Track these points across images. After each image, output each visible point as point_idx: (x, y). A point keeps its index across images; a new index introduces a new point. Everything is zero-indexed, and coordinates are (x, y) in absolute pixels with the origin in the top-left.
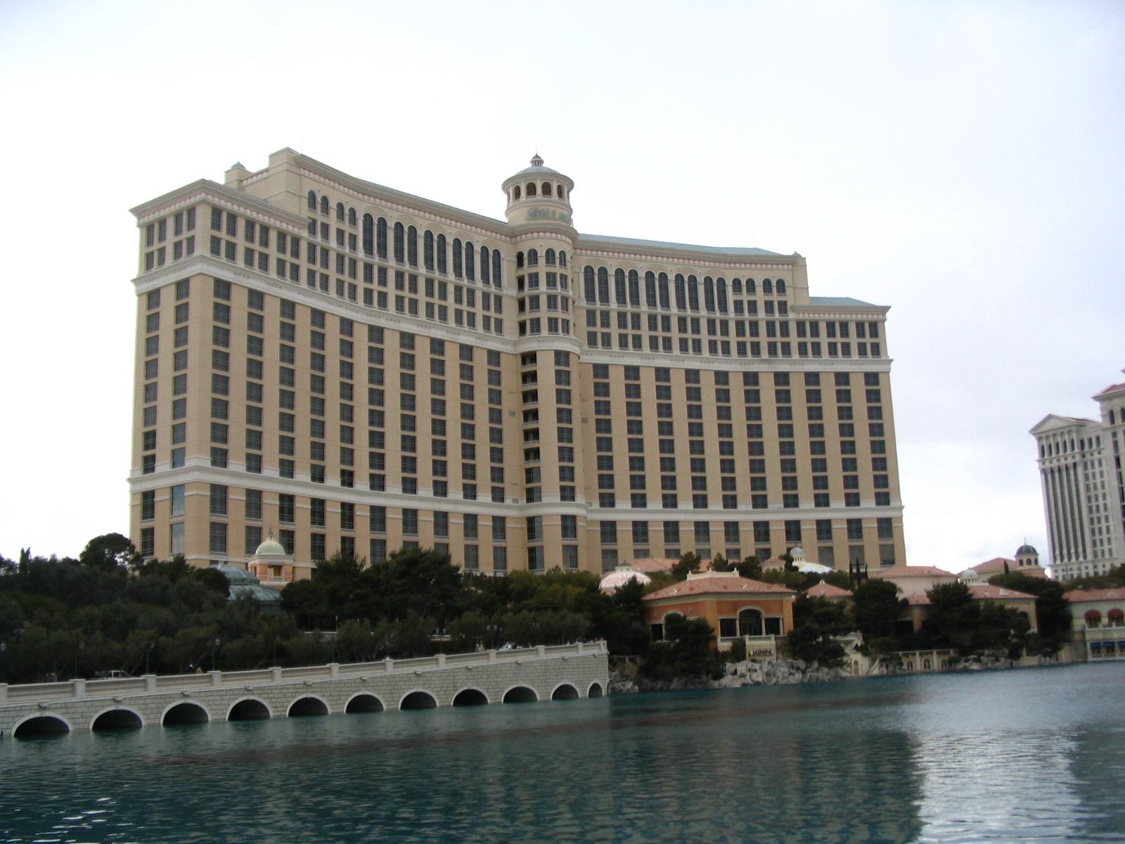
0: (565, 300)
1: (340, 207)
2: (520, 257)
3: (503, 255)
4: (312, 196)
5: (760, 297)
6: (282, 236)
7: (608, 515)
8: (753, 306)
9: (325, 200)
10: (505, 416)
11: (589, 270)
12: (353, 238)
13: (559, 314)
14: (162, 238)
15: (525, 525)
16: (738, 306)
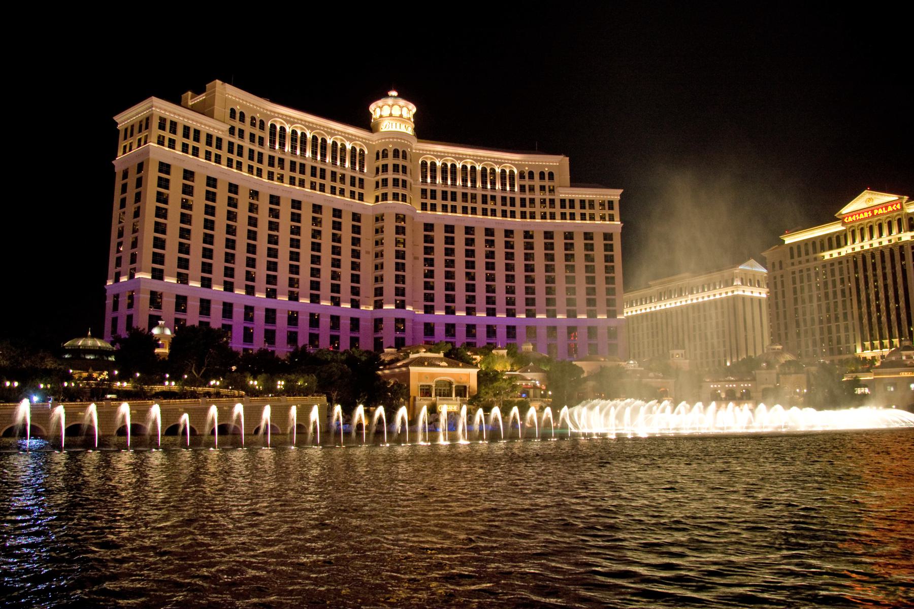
0: (404, 182)
1: (253, 119)
2: (378, 154)
3: (366, 152)
4: (233, 111)
5: (537, 182)
6: (209, 137)
7: (429, 318)
8: (532, 189)
9: (242, 115)
10: (362, 254)
11: (424, 164)
12: (261, 140)
13: (400, 191)
14: (132, 135)
15: (373, 323)
16: (522, 188)
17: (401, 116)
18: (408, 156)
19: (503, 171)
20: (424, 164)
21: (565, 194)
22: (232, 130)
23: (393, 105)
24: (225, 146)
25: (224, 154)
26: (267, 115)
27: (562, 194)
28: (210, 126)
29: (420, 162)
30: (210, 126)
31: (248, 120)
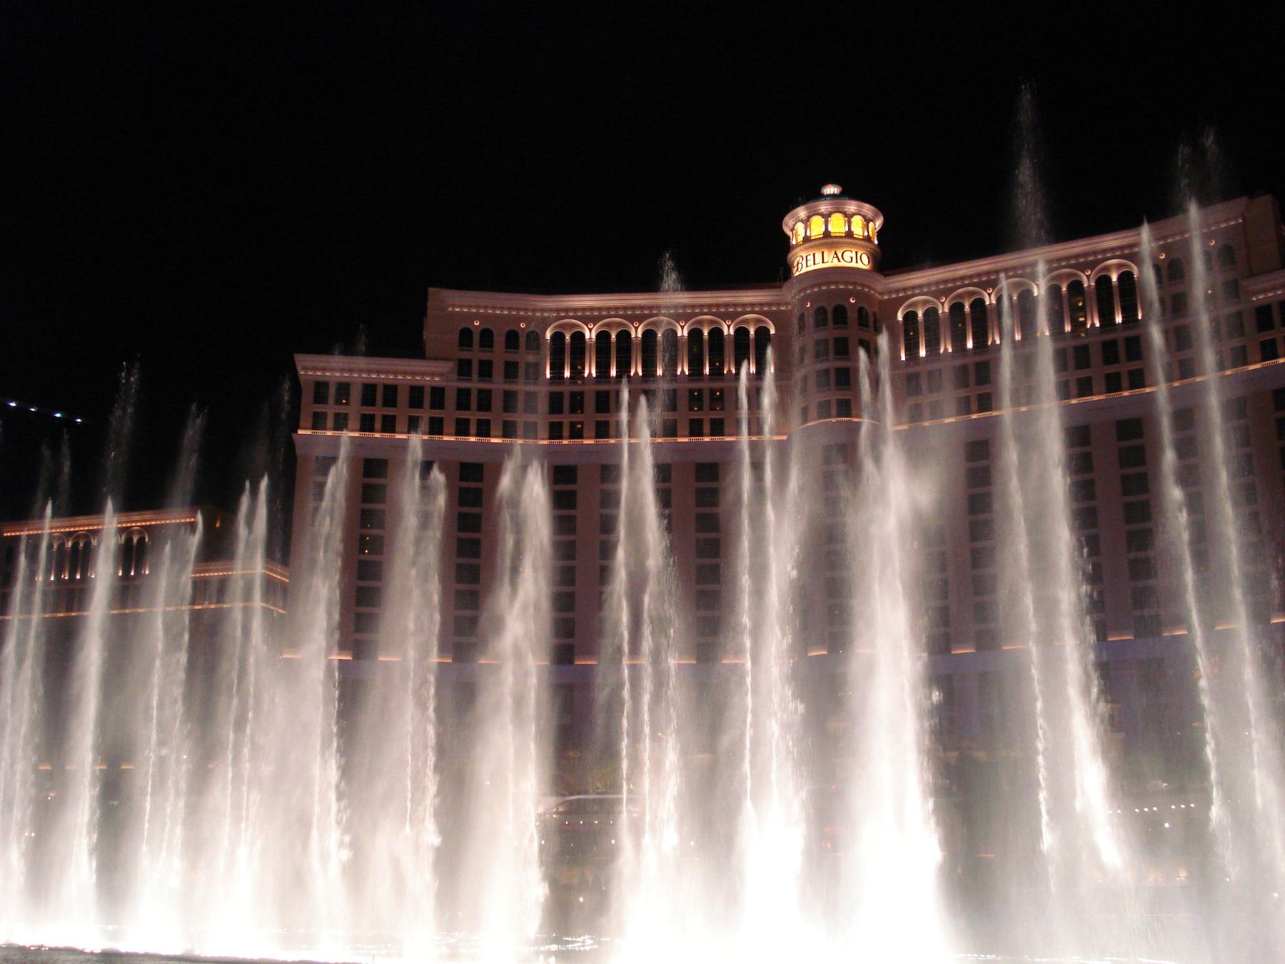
3: (772, 332)
4: (466, 335)
9: (487, 336)
11: (911, 316)
17: (827, 234)
18: (852, 316)
19: (1103, 281)
20: (911, 316)
21: (1265, 291)
22: (464, 368)
23: (809, 218)
24: (450, 400)
25: (450, 414)
26: (544, 319)
27: (1256, 293)
28: (414, 374)
29: (900, 317)
30: (414, 374)
31: (499, 340)
